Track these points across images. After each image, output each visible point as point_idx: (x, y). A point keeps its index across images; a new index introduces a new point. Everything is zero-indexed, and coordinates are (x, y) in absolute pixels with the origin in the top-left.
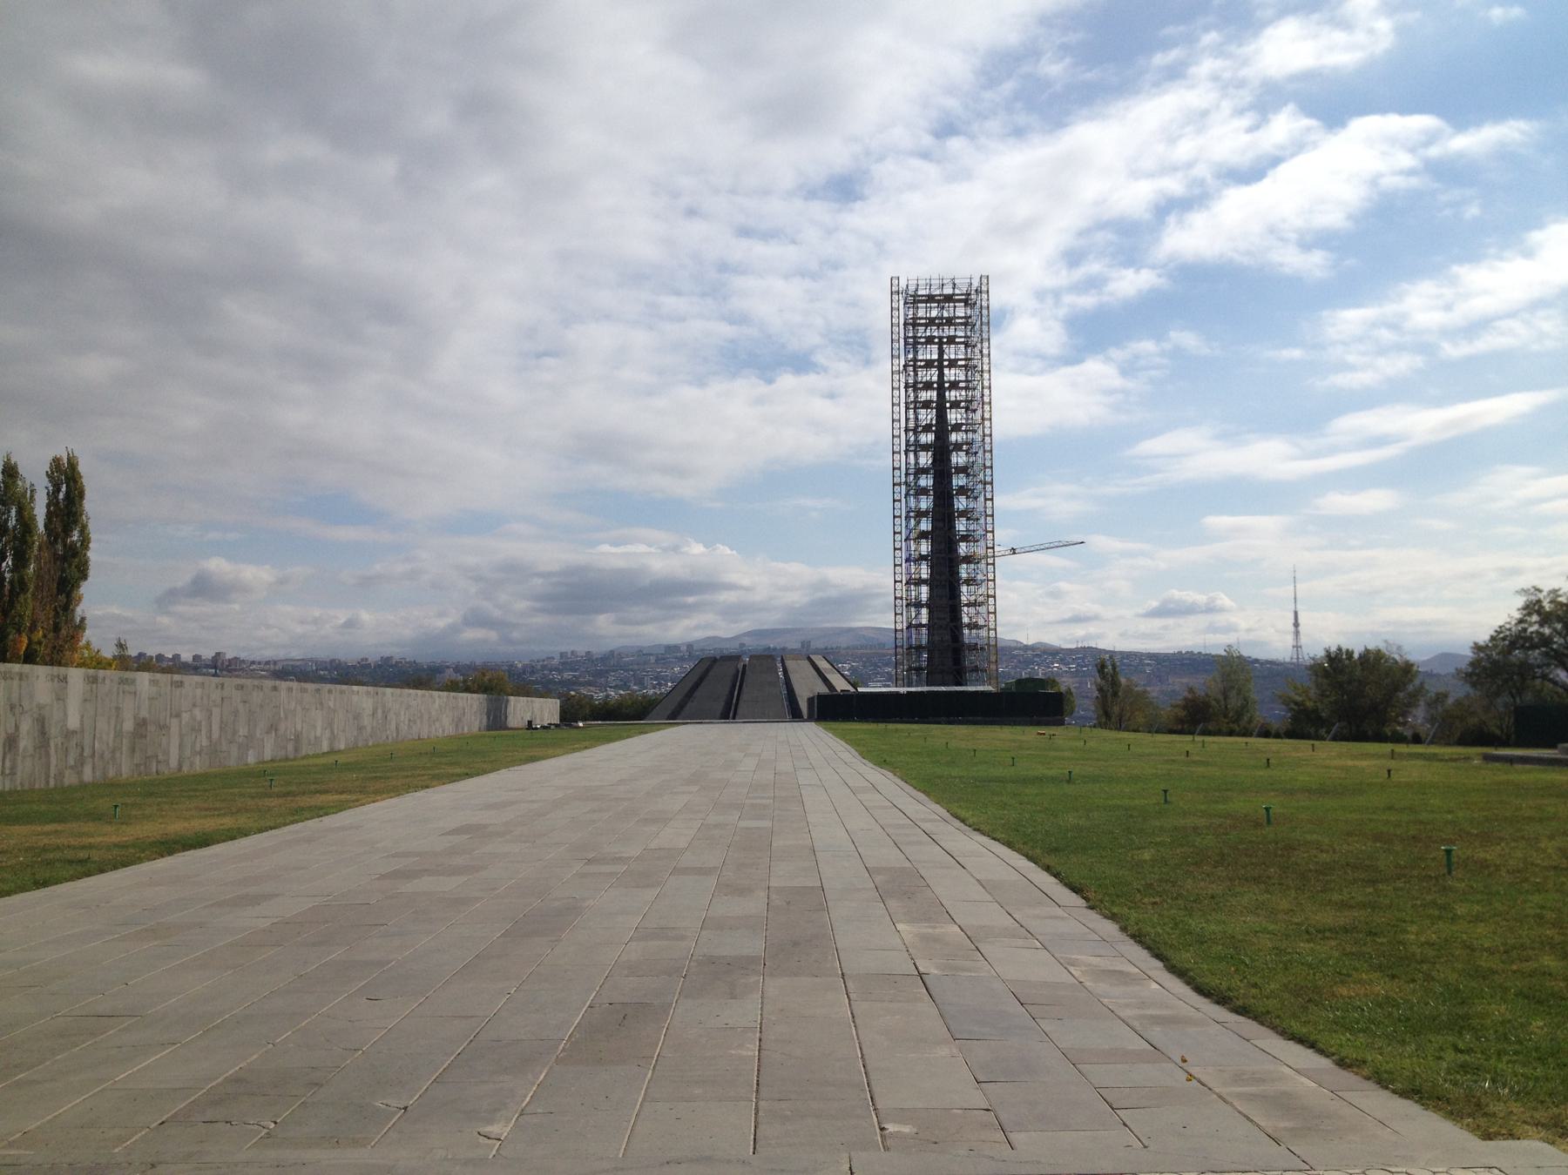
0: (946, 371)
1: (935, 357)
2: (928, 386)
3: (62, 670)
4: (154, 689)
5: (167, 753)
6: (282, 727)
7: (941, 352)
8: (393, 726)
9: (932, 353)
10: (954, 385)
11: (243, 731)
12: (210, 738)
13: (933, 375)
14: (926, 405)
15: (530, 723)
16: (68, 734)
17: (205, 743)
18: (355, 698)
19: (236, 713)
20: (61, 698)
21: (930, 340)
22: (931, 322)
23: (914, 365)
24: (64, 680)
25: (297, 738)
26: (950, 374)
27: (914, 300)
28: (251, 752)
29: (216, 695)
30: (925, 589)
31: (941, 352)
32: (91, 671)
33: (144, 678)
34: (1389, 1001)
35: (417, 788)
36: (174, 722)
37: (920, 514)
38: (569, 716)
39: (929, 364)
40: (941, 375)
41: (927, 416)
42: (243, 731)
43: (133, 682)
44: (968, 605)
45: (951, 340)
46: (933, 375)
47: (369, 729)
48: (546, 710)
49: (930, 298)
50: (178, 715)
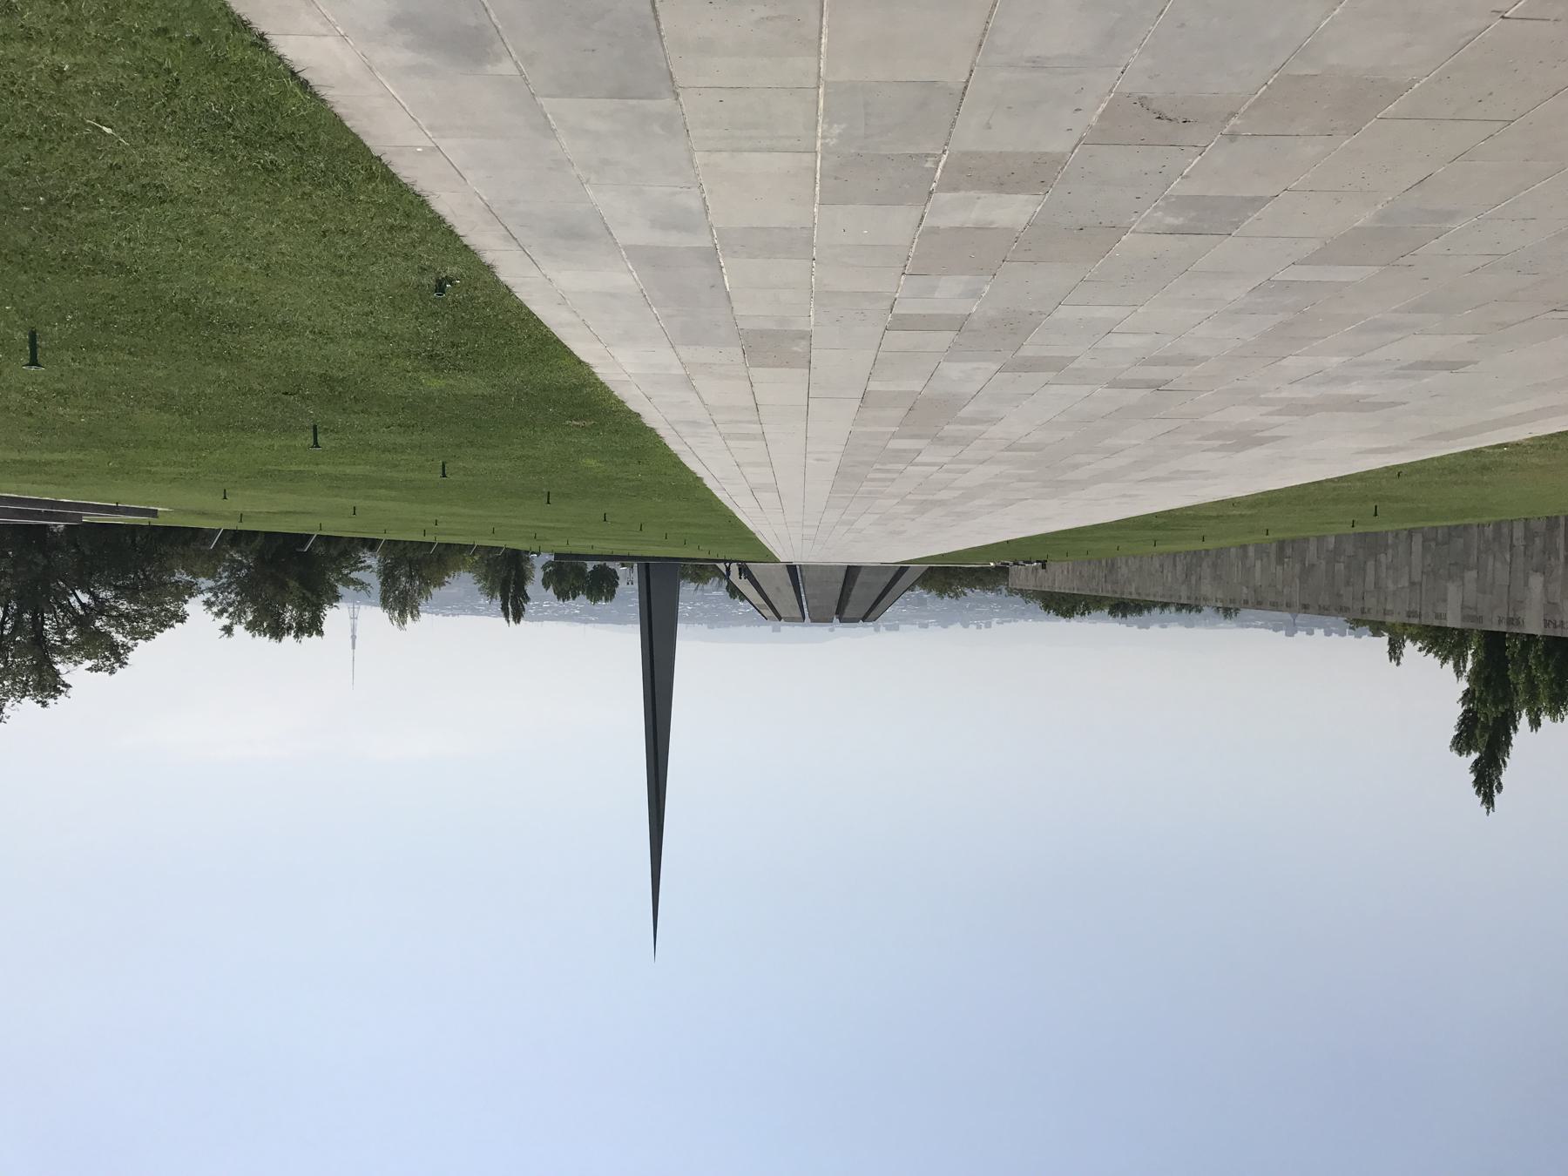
3: (1550, 632)
4: (1440, 610)
5: (1425, 549)
6: (1298, 566)
8: (1179, 568)
11: (1340, 567)
12: (1377, 563)
15: (1044, 567)
16: (1541, 569)
17: (1382, 557)
18: (1220, 595)
19: (1348, 583)
20: (1551, 606)
24: (1547, 624)
25: (1280, 561)
28: (1331, 547)
29: (1371, 602)
32: (1516, 630)
33: (1453, 621)
34: (91, 209)
35: (1331, 480)
36: (1417, 579)
38: (1003, 571)
42: (1340, 567)
43: (1464, 618)
47: (1205, 564)
48: (1022, 576)
50: (1412, 584)
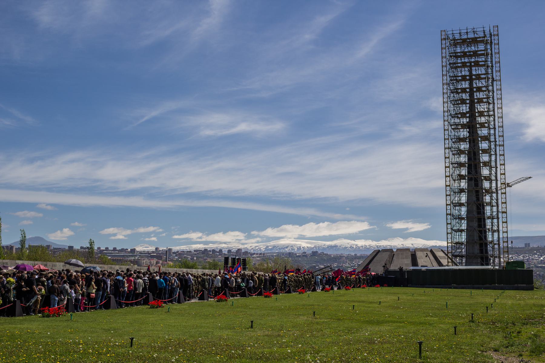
0: (467, 73)
1: (467, 73)
2: (464, 90)
7: (470, 71)
9: (465, 72)
10: (479, 89)
13: (465, 85)
14: (463, 102)
21: (464, 65)
22: (465, 54)
23: (455, 79)
26: (477, 84)
27: (455, 43)
30: (464, 210)
31: (470, 71)
37: (460, 165)
39: (464, 78)
40: (471, 84)
41: (465, 108)
44: (462, 231)
45: (477, 64)
46: (465, 85)
49: (464, 41)
